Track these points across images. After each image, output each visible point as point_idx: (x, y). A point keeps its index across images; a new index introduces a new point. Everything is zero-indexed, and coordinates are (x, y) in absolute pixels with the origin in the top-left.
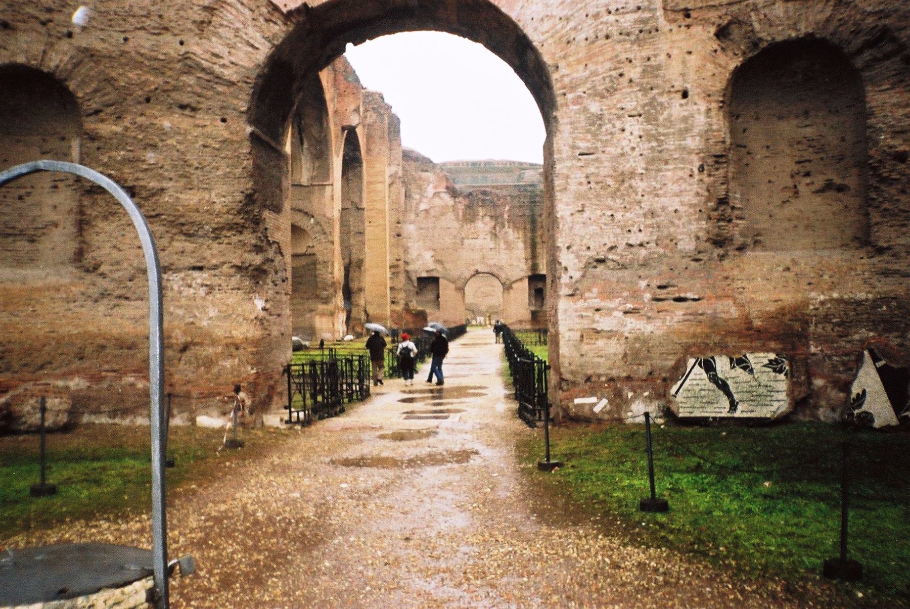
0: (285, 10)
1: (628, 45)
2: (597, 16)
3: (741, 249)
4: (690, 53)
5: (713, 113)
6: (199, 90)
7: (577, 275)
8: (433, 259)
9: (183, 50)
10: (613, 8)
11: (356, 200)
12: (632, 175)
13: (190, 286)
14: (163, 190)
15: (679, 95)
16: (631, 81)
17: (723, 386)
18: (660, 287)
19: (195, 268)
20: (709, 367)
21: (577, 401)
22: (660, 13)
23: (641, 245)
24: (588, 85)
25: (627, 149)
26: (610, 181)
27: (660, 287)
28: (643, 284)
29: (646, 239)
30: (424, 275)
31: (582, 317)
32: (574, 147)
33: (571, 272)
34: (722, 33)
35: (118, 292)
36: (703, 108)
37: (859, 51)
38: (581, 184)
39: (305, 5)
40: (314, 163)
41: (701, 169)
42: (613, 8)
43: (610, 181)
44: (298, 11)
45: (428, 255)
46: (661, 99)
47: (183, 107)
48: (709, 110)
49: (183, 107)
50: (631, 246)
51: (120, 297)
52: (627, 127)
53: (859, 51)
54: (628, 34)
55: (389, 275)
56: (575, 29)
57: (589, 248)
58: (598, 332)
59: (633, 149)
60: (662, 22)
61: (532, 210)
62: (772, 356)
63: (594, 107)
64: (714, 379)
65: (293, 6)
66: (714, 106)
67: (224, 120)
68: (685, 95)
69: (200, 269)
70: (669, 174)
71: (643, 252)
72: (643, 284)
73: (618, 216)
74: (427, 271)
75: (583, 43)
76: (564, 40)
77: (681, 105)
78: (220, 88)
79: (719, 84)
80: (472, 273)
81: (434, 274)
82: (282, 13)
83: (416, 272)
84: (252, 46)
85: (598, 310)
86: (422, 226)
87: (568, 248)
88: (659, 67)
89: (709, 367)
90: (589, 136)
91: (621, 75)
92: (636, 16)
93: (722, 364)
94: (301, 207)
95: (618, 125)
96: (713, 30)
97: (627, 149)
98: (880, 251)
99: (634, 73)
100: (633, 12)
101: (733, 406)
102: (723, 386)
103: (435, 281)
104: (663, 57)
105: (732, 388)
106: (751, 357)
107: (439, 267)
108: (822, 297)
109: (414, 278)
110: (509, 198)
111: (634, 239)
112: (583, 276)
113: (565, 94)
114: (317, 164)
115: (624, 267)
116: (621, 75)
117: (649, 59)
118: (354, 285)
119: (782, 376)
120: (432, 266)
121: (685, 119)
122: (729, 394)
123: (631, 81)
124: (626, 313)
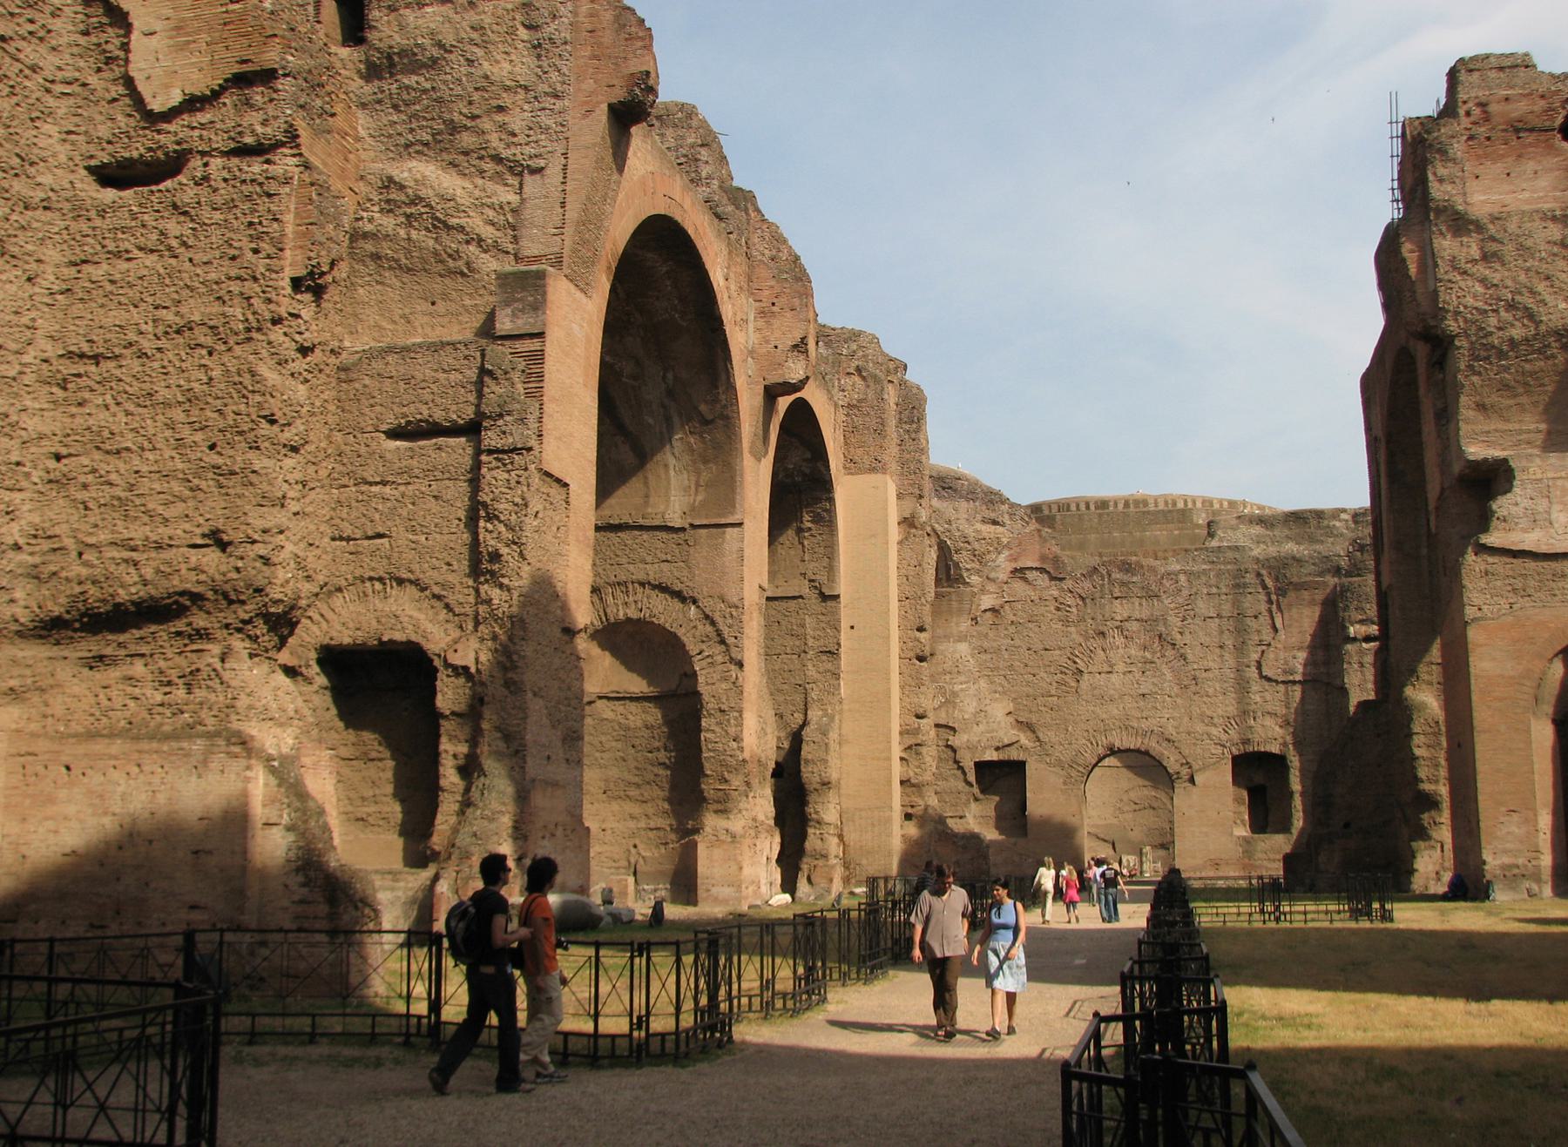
8: (1011, 719)
11: (822, 577)
30: (991, 756)
40: (698, 473)
45: (999, 710)
55: (897, 751)
61: (1236, 604)
74: (997, 749)
80: (1101, 751)
81: (1014, 754)
83: (971, 748)
86: (986, 645)
94: (667, 580)
103: (1018, 768)
107: (1025, 739)
109: (969, 765)
110: (1182, 578)
114: (705, 476)
118: (810, 774)
120: (1008, 733)
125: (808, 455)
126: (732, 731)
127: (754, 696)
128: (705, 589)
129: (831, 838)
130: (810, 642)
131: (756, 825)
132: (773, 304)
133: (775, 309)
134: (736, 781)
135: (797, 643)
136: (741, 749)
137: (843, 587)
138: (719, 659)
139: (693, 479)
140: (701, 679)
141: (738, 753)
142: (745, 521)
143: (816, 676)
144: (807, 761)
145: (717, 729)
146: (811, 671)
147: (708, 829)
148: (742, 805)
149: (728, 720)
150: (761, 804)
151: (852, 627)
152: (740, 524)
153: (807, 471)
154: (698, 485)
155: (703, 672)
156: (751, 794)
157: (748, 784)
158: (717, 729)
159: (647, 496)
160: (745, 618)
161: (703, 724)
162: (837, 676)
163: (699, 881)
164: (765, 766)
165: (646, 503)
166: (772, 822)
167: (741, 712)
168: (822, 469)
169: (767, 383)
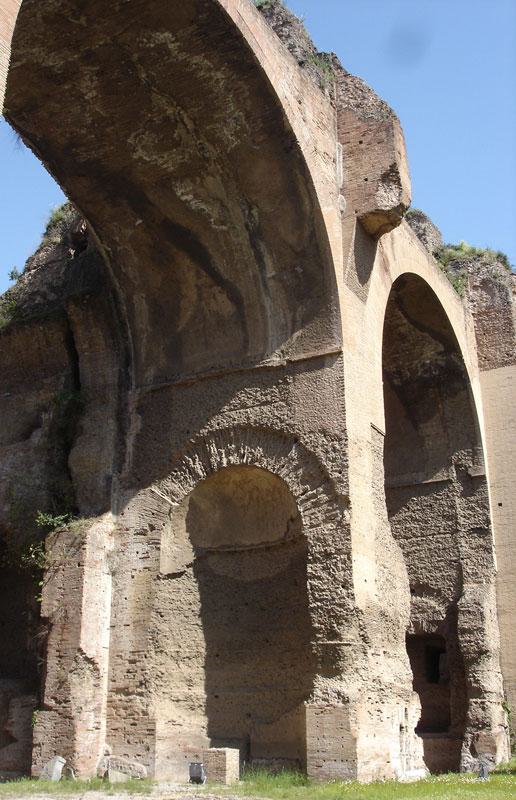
40: (293, 310)
125: (441, 348)
126: (340, 575)
127: (370, 539)
128: (305, 424)
129: (493, 706)
130: (461, 520)
131: (382, 690)
132: (361, 142)
133: (363, 146)
134: (350, 634)
135: (450, 523)
136: (352, 596)
137: (488, 469)
138: (324, 497)
139: (289, 316)
140: (306, 521)
141: (348, 601)
142: (344, 349)
143: (470, 551)
144: (464, 631)
145: (324, 575)
146: (465, 548)
147: (318, 692)
148: (358, 664)
149: (336, 565)
150: (394, 666)
151: (500, 505)
152: (340, 353)
153: (443, 364)
154: (294, 321)
155: (307, 513)
156: (370, 651)
157: (364, 638)
158: (324, 575)
159: (246, 341)
160: (351, 451)
161: (309, 570)
162: (488, 550)
163: (309, 755)
164: (396, 624)
165: (245, 348)
166: (409, 687)
167: (349, 554)
168: (456, 360)
169: (359, 214)
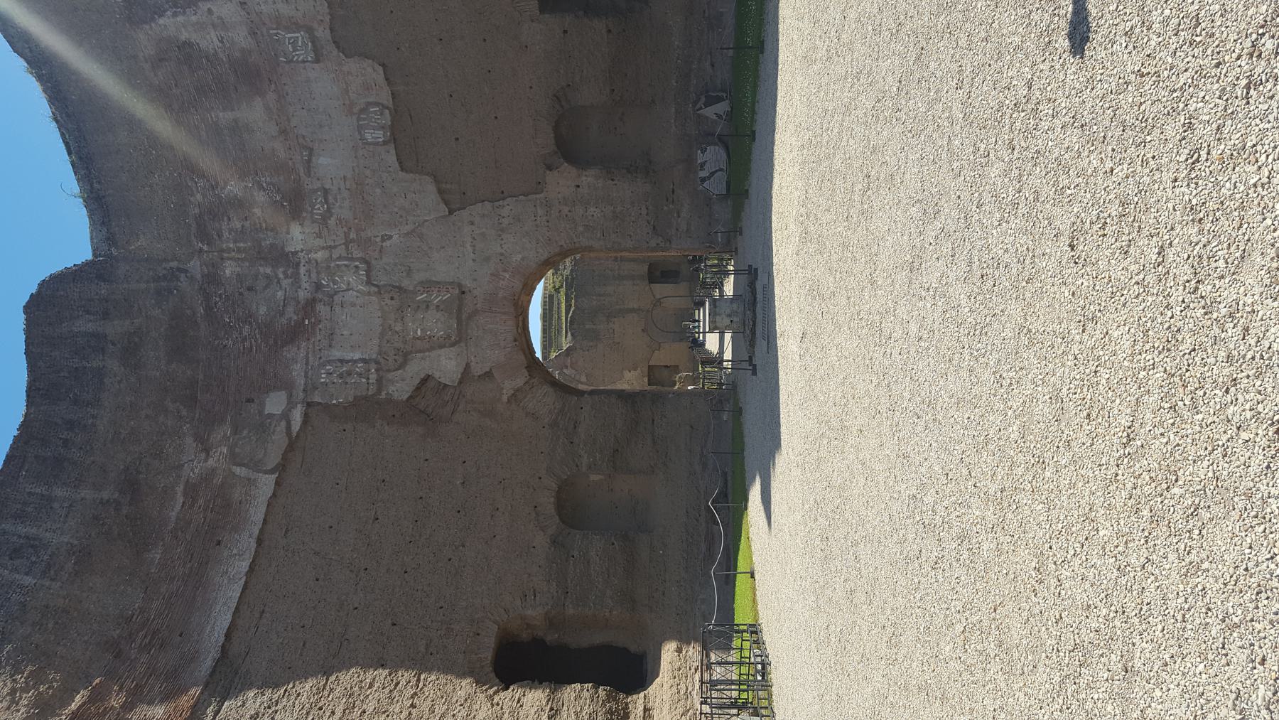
0: (529, 377)
1: (553, 212)
2: (537, 226)
3: (650, 162)
4: (558, 183)
5: (587, 173)
6: (567, 419)
7: (660, 238)
9: (546, 426)
10: (533, 218)
12: (614, 212)
13: (661, 425)
14: (615, 436)
15: (578, 189)
16: (570, 211)
17: (712, 174)
18: (667, 201)
19: (653, 423)
20: (703, 180)
21: (720, 240)
22: (538, 196)
23: (647, 209)
24: (570, 231)
25: (602, 214)
26: (617, 222)
27: (667, 201)
28: (665, 208)
29: (644, 206)
31: (680, 237)
32: (599, 239)
33: (659, 242)
34: (550, 168)
35: (664, 457)
36: (584, 178)
37: (562, 107)
38: (617, 236)
39: (526, 368)
41: (613, 180)
42: (533, 218)
43: (617, 222)
44: (528, 371)
46: (579, 198)
47: (575, 427)
48: (586, 176)
49: (575, 427)
50: (647, 215)
51: (666, 457)
52: (591, 214)
53: (562, 107)
54: (547, 212)
56: (543, 237)
57: (648, 233)
58: (688, 230)
59: (602, 211)
60: (541, 195)
62: (699, 152)
63: (581, 229)
64: (709, 178)
65: (527, 374)
66: (584, 173)
67: (582, 408)
68: (578, 186)
69: (653, 420)
70: (614, 195)
71: (650, 207)
72: (665, 208)
73: (633, 219)
75: (550, 233)
76: (548, 242)
77: (583, 188)
78: (566, 409)
79: (574, 171)
82: (530, 379)
84: (545, 395)
85: (677, 230)
87: (648, 243)
88: (564, 198)
89: (703, 180)
90: (595, 232)
91: (566, 216)
92: (538, 207)
93: (703, 174)
95: (590, 218)
96: (548, 172)
97: (602, 214)
98: (653, 101)
99: (566, 210)
100: (536, 209)
101: (721, 170)
102: (712, 174)
104: (560, 195)
105: (714, 170)
106: (699, 162)
108: (674, 127)
111: (644, 212)
112: (661, 236)
113: (574, 243)
115: (657, 217)
116: (566, 216)
117: (560, 202)
119: (708, 148)
121: (589, 187)
122: (716, 171)
123: (570, 211)
124: (679, 217)
